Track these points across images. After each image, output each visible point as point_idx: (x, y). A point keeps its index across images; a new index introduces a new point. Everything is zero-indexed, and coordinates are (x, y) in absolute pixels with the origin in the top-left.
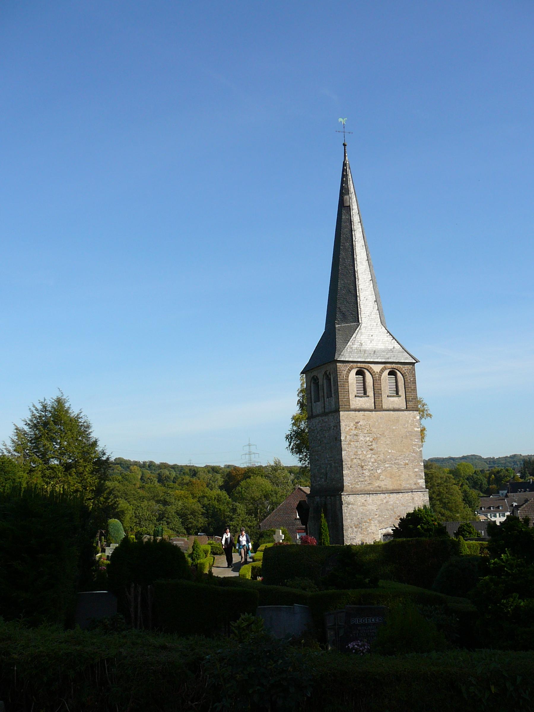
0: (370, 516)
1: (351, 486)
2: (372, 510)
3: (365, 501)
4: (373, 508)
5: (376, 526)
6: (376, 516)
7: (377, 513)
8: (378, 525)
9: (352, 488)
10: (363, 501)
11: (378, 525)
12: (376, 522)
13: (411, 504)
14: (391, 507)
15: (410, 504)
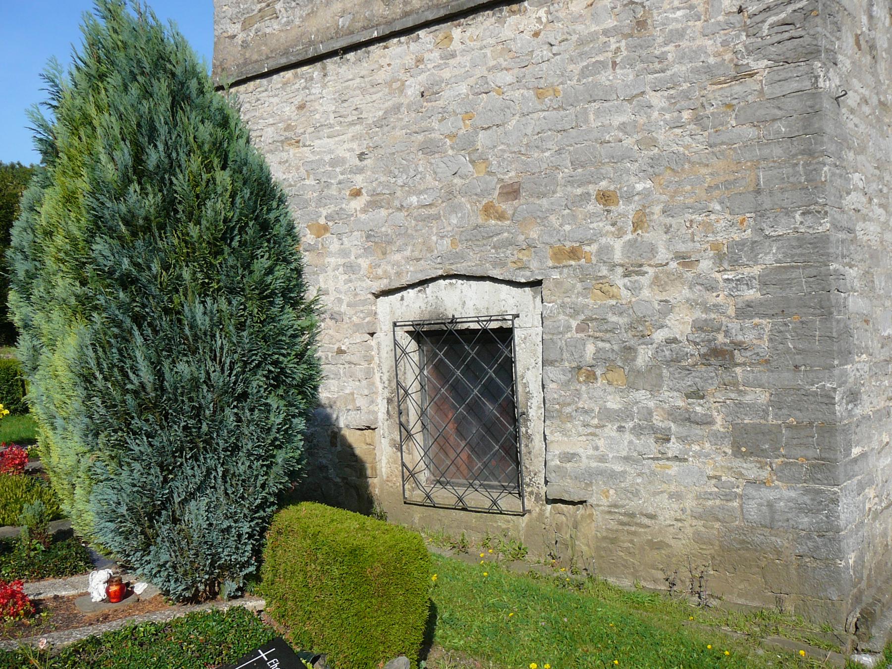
0: (321, 201)
1: (241, 37)
2: (334, 163)
3: (301, 107)
4: (341, 153)
5: (350, 268)
6: (357, 204)
7: (359, 181)
8: (364, 263)
9: (245, 45)
10: (289, 110)
11: (364, 263)
12: (354, 241)
13: (624, 76)
14: (449, 126)
15: (605, 77)
